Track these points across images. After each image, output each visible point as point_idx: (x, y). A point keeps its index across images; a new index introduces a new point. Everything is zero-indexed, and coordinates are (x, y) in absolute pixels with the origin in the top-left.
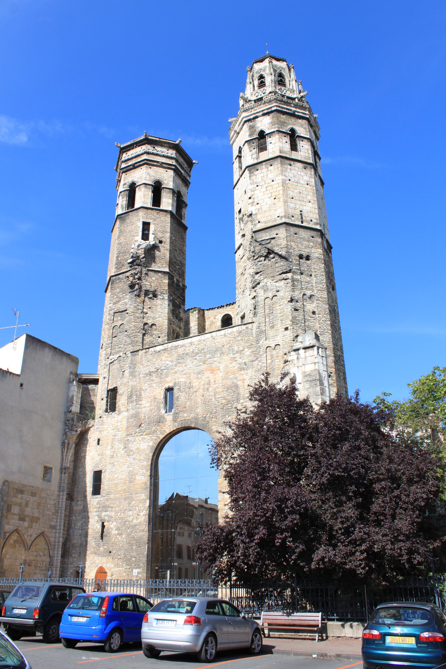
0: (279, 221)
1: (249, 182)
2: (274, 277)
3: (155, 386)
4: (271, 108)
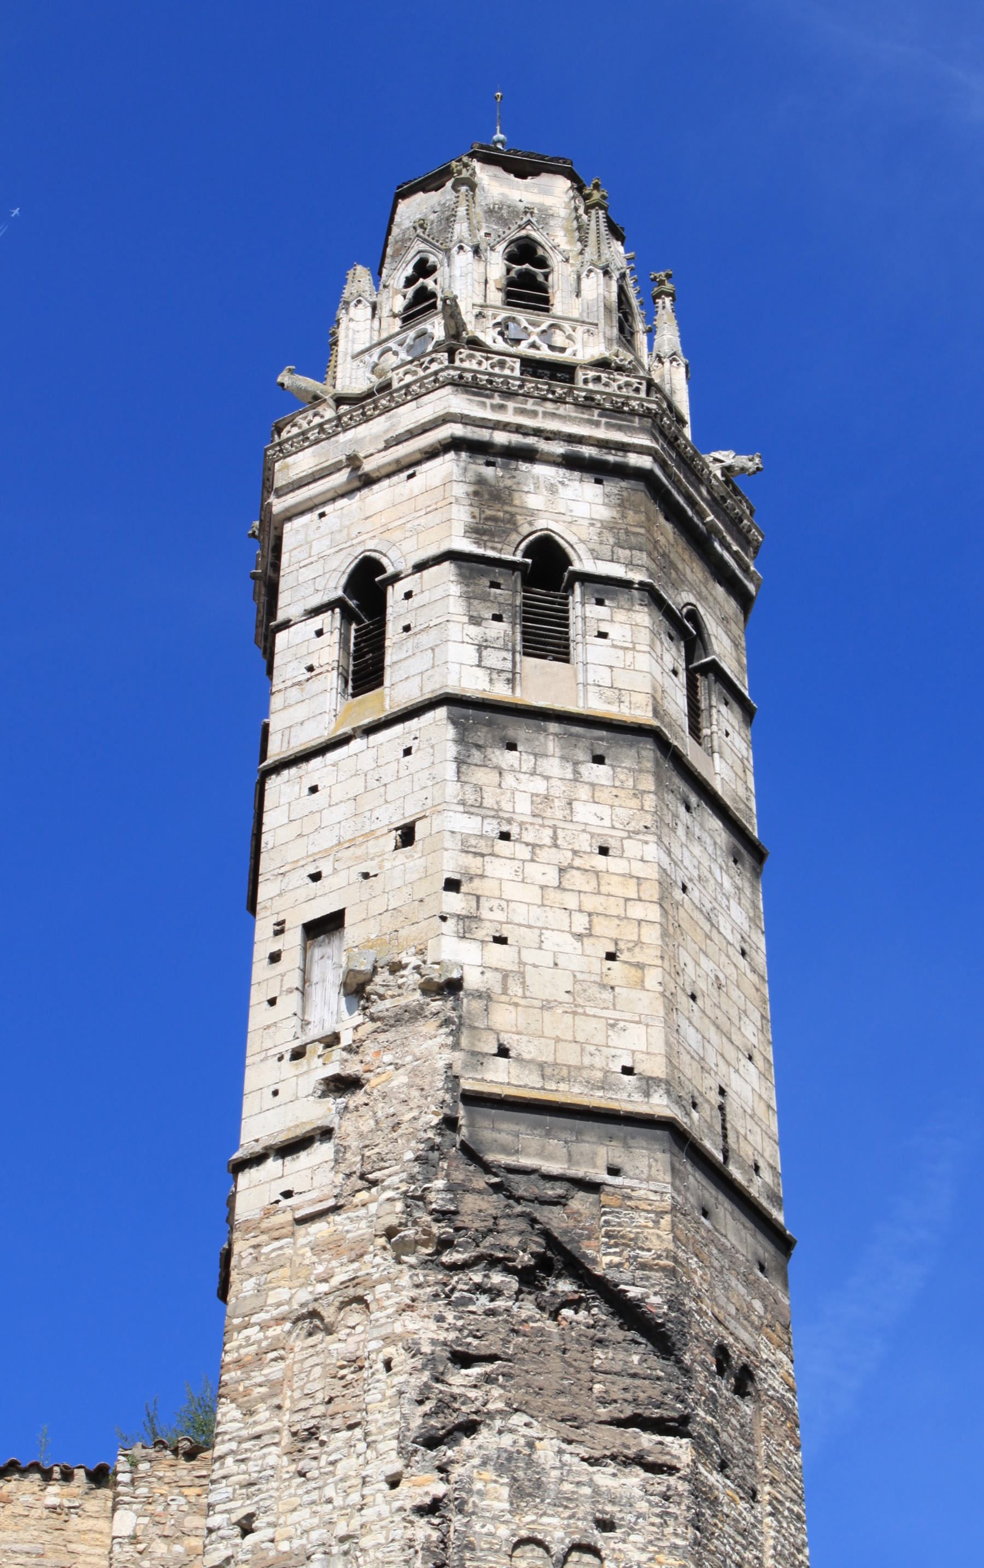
0: (628, 1098)
1: (452, 789)
2: (574, 1421)
4: (624, 448)
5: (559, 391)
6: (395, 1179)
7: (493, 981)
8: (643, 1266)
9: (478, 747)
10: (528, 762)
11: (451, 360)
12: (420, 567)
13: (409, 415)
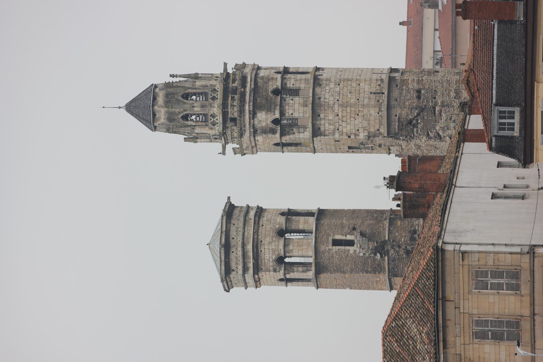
1: (330, 137)
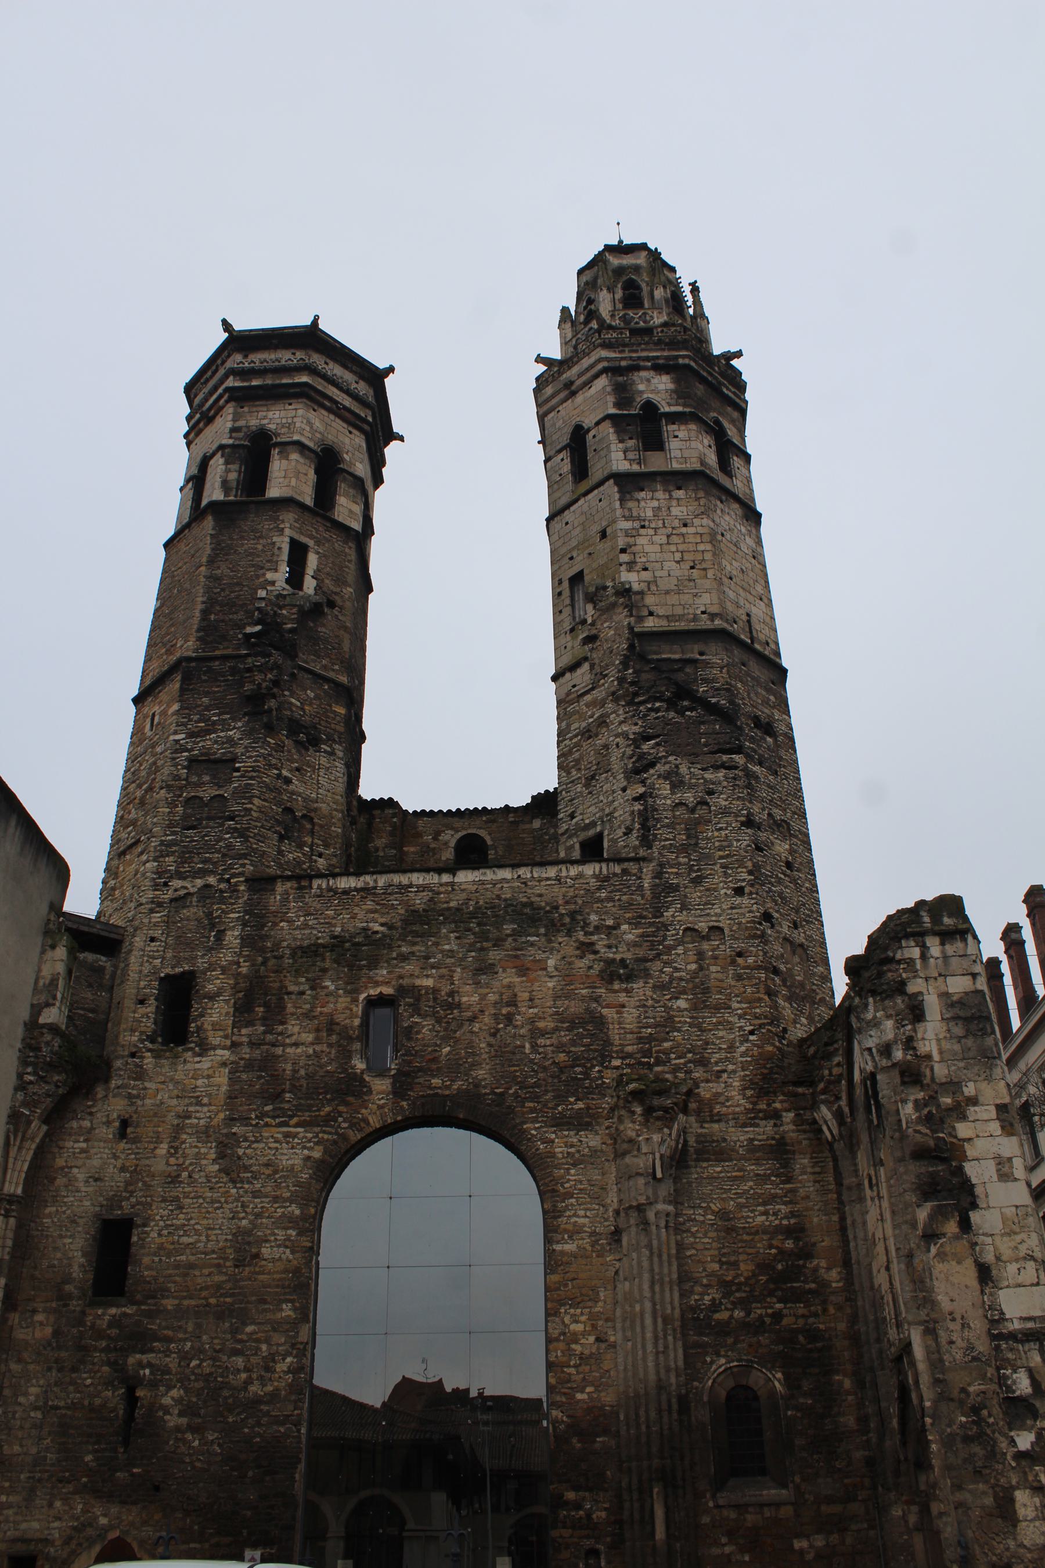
0: (705, 623)
1: (619, 512)
3: (332, 988)
4: (677, 357)
5: (646, 339)
6: (613, 673)
7: (644, 586)
8: (717, 689)
9: (629, 493)
10: (650, 495)
11: (600, 336)
12: (597, 424)
13: (586, 362)
